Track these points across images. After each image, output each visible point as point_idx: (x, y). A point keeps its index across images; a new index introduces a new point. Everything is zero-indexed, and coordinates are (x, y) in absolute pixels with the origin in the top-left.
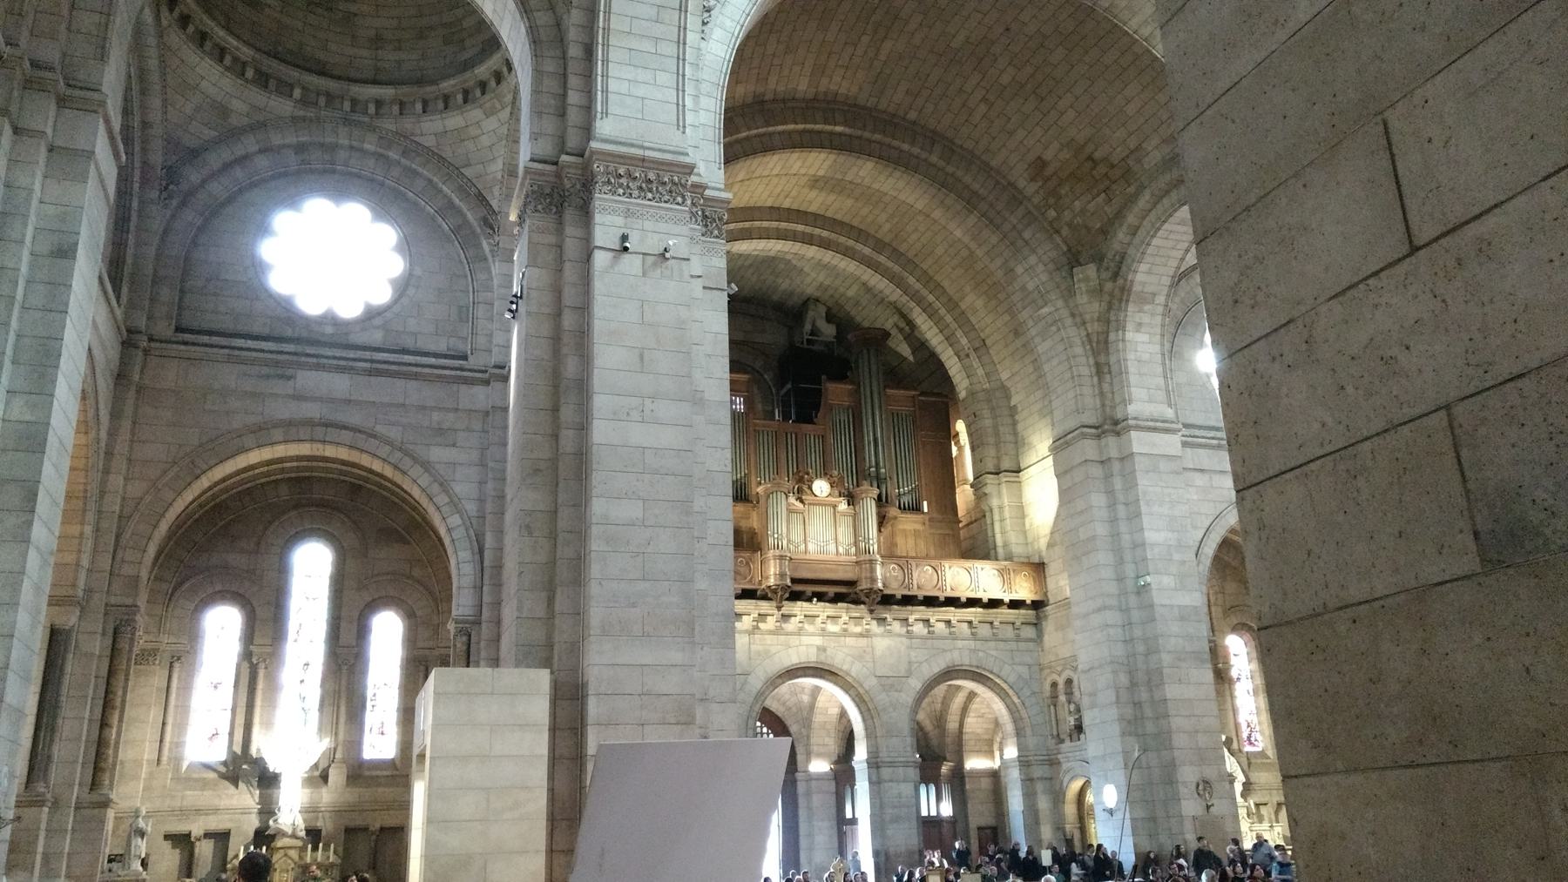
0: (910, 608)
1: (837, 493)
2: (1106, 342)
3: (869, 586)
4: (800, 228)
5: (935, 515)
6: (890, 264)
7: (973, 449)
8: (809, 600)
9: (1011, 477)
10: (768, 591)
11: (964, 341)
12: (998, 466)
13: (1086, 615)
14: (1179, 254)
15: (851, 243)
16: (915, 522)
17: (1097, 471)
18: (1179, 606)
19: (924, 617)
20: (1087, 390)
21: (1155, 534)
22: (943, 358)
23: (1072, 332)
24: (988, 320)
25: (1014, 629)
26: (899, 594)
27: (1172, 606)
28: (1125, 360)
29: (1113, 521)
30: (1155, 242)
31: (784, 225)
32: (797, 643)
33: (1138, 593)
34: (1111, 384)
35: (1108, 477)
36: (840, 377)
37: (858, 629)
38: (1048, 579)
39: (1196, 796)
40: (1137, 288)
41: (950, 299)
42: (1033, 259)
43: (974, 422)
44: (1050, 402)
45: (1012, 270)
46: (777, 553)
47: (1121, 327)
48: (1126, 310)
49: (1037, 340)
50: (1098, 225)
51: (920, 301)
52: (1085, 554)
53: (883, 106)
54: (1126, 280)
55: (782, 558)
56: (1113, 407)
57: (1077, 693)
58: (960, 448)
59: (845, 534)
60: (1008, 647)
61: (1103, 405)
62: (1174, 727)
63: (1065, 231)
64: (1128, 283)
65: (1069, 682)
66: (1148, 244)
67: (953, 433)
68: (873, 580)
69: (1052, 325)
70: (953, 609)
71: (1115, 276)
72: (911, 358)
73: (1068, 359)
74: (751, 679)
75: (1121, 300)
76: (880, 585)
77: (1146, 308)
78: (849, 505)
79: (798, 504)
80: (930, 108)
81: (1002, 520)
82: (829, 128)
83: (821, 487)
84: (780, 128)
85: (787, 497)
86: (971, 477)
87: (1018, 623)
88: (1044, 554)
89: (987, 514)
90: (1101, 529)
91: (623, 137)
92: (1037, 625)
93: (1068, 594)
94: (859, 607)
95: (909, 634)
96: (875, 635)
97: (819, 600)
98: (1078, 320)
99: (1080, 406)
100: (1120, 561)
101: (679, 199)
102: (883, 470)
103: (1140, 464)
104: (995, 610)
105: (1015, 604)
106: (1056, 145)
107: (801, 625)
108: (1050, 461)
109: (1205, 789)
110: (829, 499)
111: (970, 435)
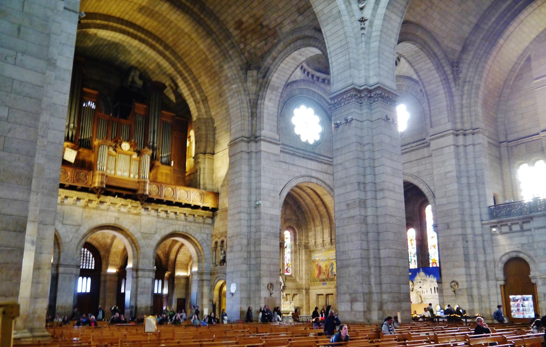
0: (160, 205)
1: (132, 149)
2: (257, 104)
3: (142, 192)
5: (176, 168)
7: (196, 143)
8: (114, 196)
9: (210, 156)
10: (94, 189)
11: (198, 96)
12: (205, 151)
13: (234, 214)
14: (290, 72)
17: (245, 156)
18: (270, 214)
19: (166, 210)
20: (246, 123)
21: (265, 185)
22: (188, 102)
23: (243, 97)
24: (210, 89)
26: (156, 198)
27: (267, 214)
28: (263, 112)
29: (250, 177)
30: (282, 65)
33: (255, 208)
34: (256, 121)
35: (250, 159)
36: (142, 100)
37: (135, 212)
38: (220, 200)
39: (267, 289)
40: (272, 83)
41: (195, 77)
42: (232, 64)
43: (198, 131)
44: (231, 126)
46: (101, 172)
47: (263, 98)
48: (266, 92)
49: (229, 99)
50: (260, 54)
51: (182, 75)
52: (237, 189)
54: (268, 79)
55: (103, 175)
56: (256, 131)
57: (225, 247)
58: (190, 143)
59: (134, 167)
61: (252, 129)
62: (262, 262)
63: (246, 54)
64: (269, 81)
65: (222, 242)
66: (279, 65)
67: (188, 136)
68: (145, 190)
69: (236, 93)
70: (178, 207)
71: (264, 77)
72: (174, 101)
73: (240, 108)
74: (81, 228)
75: (265, 87)
76: (147, 193)
77: (274, 92)
78: (138, 156)
79: (114, 152)
81: (204, 174)
83: (126, 146)
85: (109, 148)
86: (193, 155)
87: (205, 217)
88: (219, 189)
89: (198, 171)
90: (244, 180)
92: (213, 217)
93: (227, 206)
94: (137, 202)
95: (158, 216)
96: (143, 215)
98: (247, 93)
99: (243, 128)
100: (250, 194)
102: (155, 145)
103: (263, 155)
104: (196, 210)
105: (205, 208)
106: (248, 16)
107: (108, 207)
108: (228, 149)
109: (271, 287)
111: (196, 137)
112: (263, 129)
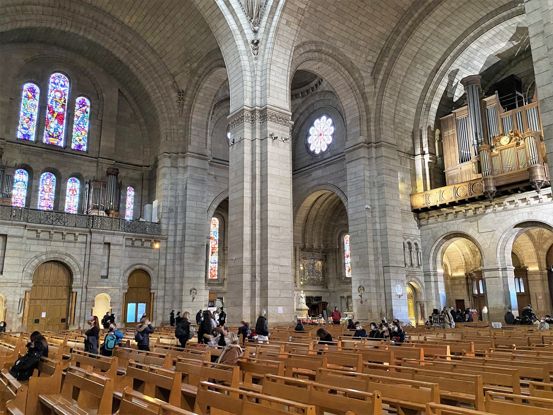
4: (504, 14)
32: (517, 212)
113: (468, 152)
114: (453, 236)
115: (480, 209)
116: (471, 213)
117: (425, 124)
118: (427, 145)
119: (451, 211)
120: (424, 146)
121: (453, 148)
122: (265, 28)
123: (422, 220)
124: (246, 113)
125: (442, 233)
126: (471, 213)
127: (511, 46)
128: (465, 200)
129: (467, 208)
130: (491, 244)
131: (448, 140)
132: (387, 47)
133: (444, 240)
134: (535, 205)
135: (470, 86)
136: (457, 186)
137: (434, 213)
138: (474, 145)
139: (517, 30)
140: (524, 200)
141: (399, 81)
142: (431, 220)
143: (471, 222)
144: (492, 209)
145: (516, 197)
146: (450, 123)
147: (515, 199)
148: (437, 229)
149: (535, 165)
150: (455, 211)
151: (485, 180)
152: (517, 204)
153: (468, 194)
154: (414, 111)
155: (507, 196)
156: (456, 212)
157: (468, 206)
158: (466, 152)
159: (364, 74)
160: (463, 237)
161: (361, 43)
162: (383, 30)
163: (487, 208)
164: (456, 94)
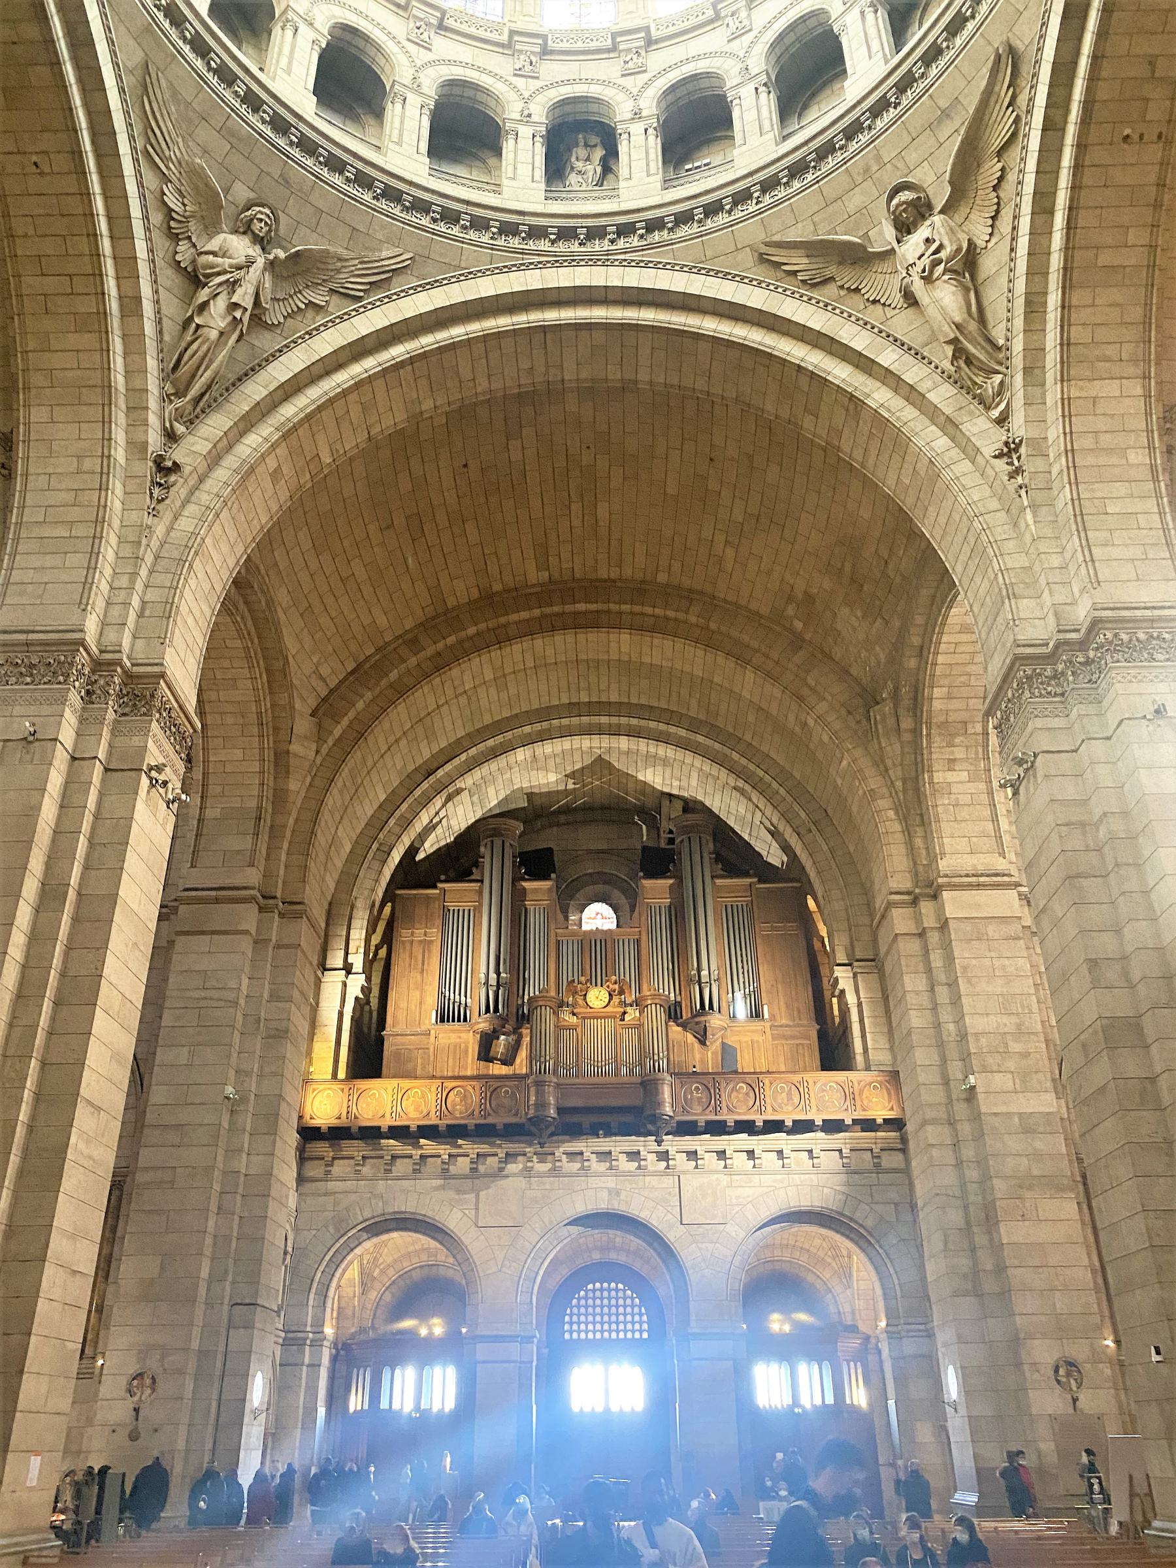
4: (604, 720)
6: (709, 742)
15: (662, 727)
16: (753, 1031)
25: (873, 1157)
27: (1009, 1115)
31: (585, 719)
41: (782, 770)
42: (822, 707)
45: (806, 723)
53: (628, 572)
60: (863, 1182)
70: (784, 1135)
80: (676, 566)
82: (569, 608)
84: (514, 617)
91: (25, 623)
97: (605, 1136)
101: (61, 679)
102: (704, 973)
109: (1068, 1375)
110: (609, 1009)
112: (943, 854)
113: (463, 998)
114: (393, 1225)
115: (490, 1160)
116: (463, 1164)
117: (366, 893)
118: (362, 950)
119: (409, 1150)
120: (352, 949)
121: (419, 976)
122: (215, 446)
123: (309, 1165)
124: (82, 657)
125: (367, 1214)
126: (463, 1164)
127: (561, 787)
128: (465, 1126)
129: (455, 1151)
130: (506, 1262)
131: (407, 954)
132: (375, 666)
133: (365, 1236)
134: (629, 1174)
135: (498, 842)
136: (450, 1084)
137: (355, 1148)
138: (487, 983)
139: (595, 761)
140: (605, 1156)
141: (370, 763)
142: (339, 1168)
143: (458, 1192)
144: (521, 1166)
145: (587, 1146)
146: (420, 911)
147: (584, 1149)
148: (353, 1197)
149: (660, 1075)
150: (419, 1152)
151: (539, 1084)
152: (586, 1164)
153: (432, 1114)
154: (348, 847)
155: (567, 1137)
156: (421, 1156)
157: (460, 1146)
158: (457, 997)
159: (298, 705)
160: (424, 1234)
161: (324, 620)
162: (382, 621)
163: (510, 1159)
164: (427, 845)
